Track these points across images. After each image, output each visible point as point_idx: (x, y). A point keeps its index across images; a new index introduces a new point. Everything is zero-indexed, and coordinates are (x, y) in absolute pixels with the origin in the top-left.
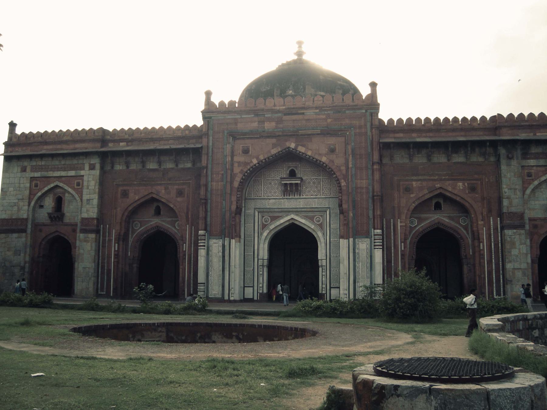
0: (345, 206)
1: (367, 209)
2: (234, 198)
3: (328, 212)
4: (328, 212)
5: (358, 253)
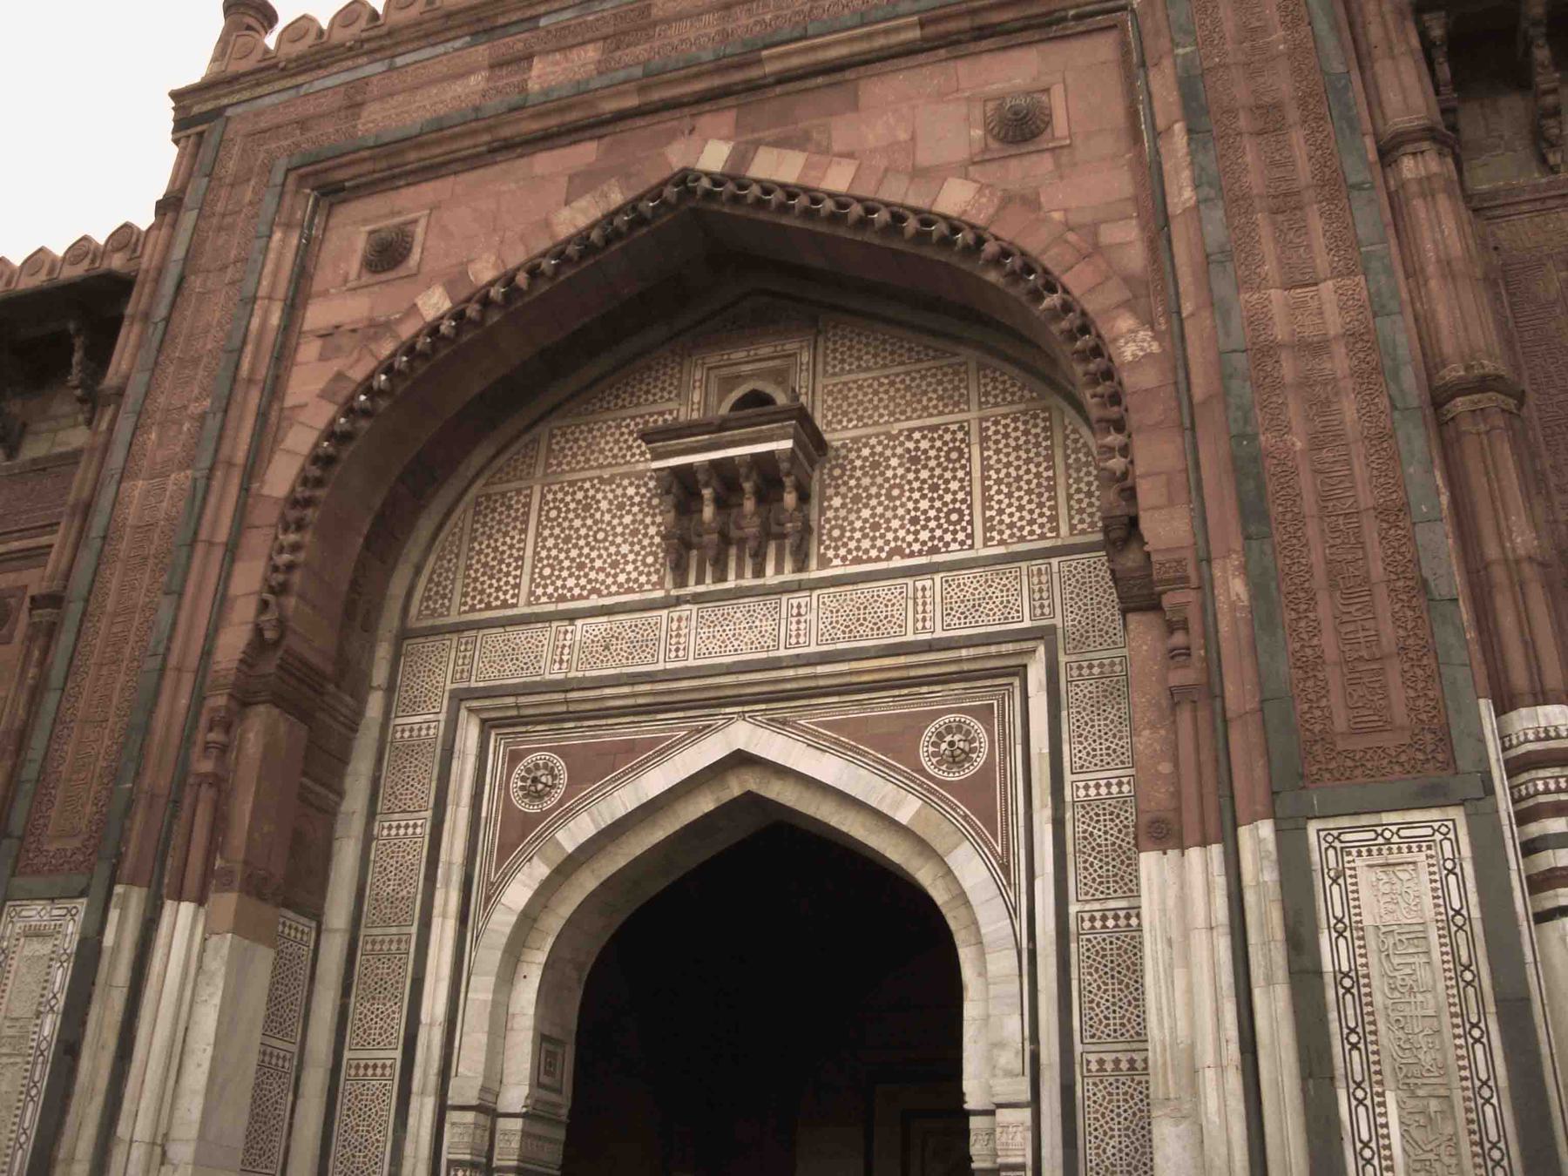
0: (1164, 528)
1: (1395, 513)
2: (248, 578)
3: (1037, 673)
4: (1037, 673)
5: (1354, 982)
